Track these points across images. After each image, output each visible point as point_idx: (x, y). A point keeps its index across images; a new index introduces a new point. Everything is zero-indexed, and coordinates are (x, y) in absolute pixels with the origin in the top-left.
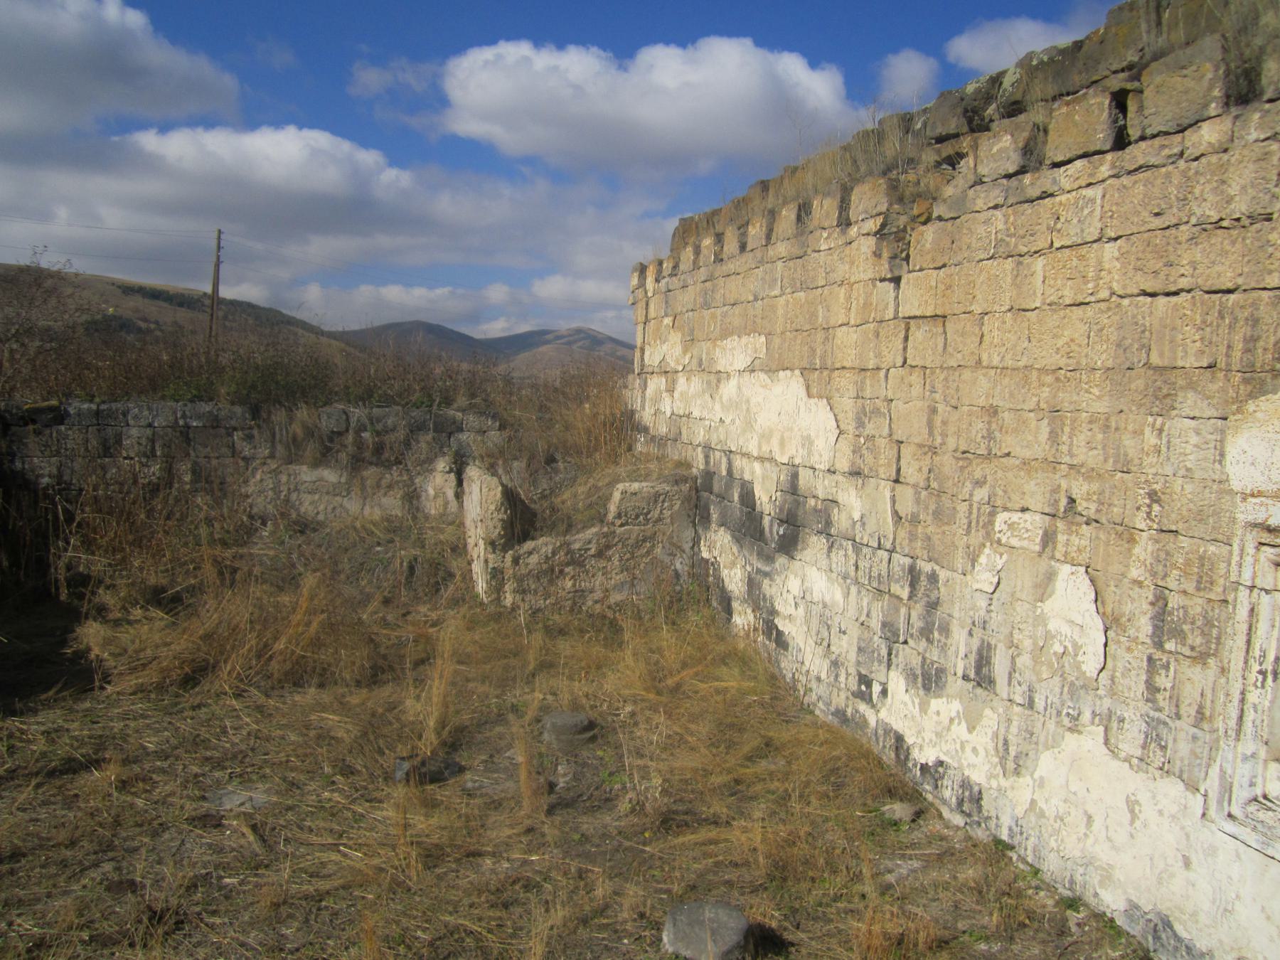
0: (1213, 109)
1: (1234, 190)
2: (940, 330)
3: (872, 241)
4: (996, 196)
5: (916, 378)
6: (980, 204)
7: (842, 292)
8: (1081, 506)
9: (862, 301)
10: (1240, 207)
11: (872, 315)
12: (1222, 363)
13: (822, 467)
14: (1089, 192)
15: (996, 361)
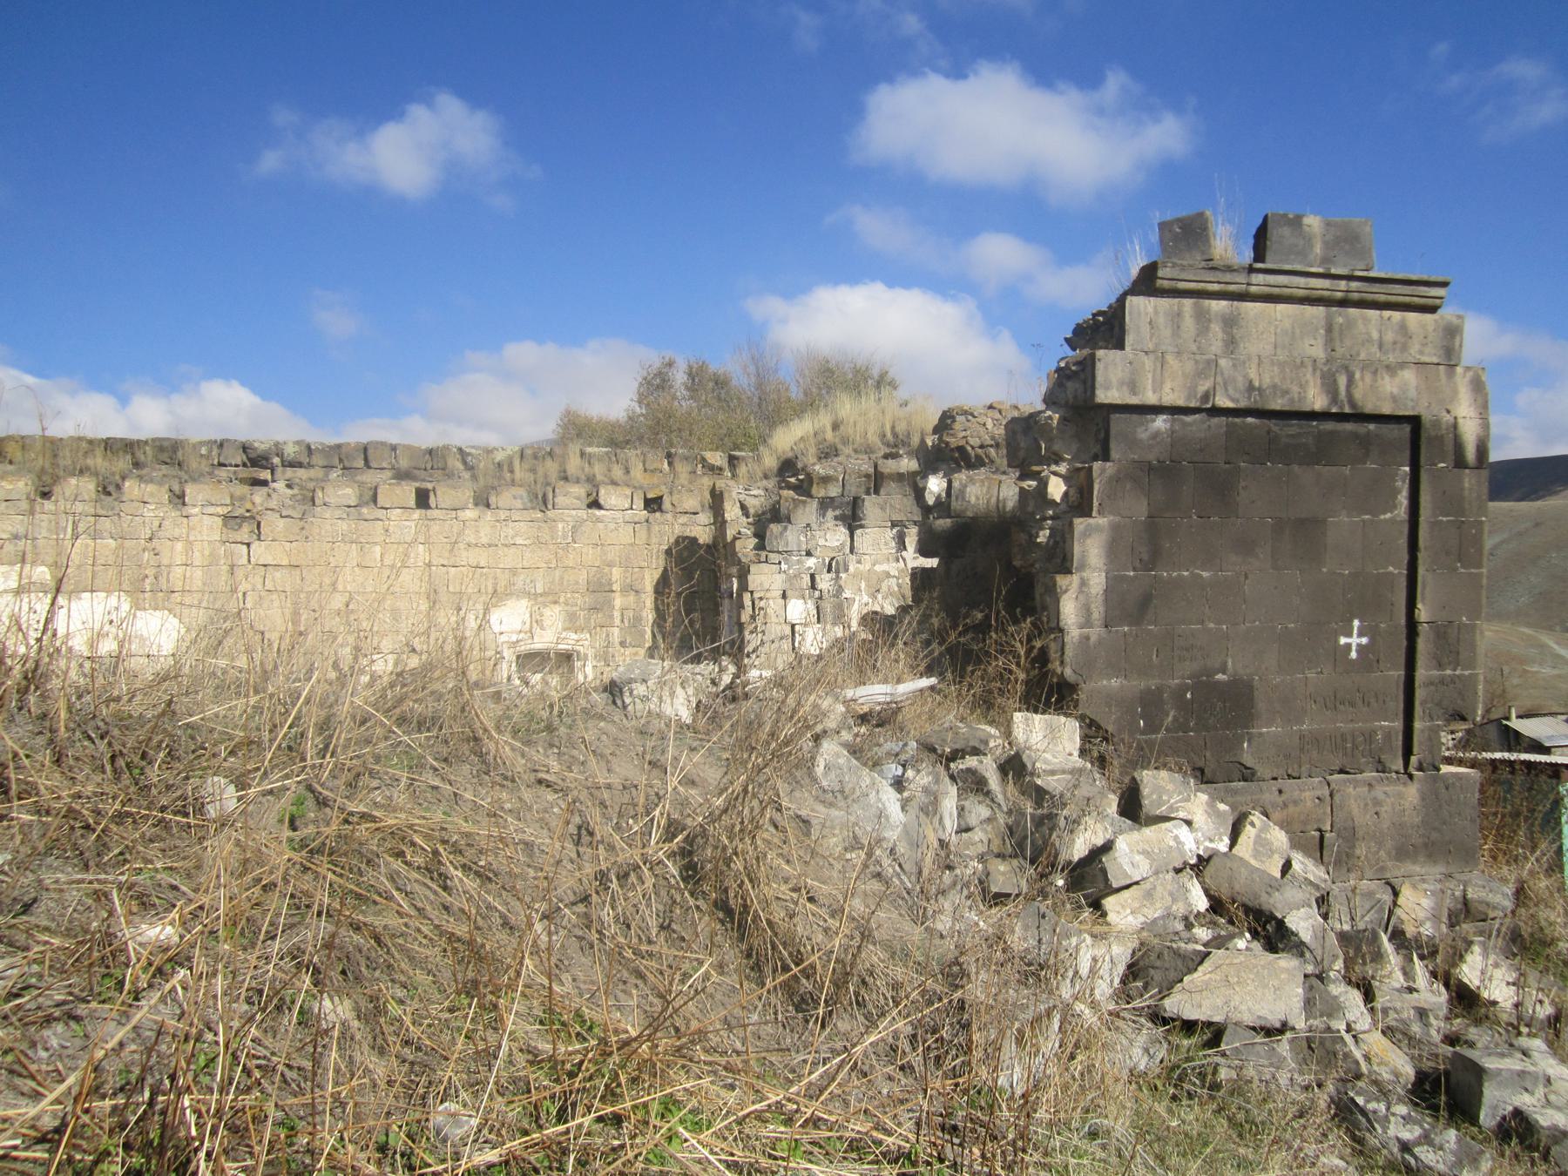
0: (470, 506)
1: (482, 534)
2: (298, 573)
3: (219, 521)
4: (338, 513)
5: (275, 596)
6: (327, 516)
7: (179, 546)
8: (418, 648)
9: (207, 553)
10: (484, 540)
11: (222, 562)
12: (483, 590)
13: (165, 653)
14: (407, 523)
15: (349, 588)
